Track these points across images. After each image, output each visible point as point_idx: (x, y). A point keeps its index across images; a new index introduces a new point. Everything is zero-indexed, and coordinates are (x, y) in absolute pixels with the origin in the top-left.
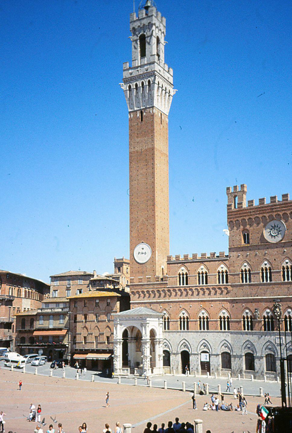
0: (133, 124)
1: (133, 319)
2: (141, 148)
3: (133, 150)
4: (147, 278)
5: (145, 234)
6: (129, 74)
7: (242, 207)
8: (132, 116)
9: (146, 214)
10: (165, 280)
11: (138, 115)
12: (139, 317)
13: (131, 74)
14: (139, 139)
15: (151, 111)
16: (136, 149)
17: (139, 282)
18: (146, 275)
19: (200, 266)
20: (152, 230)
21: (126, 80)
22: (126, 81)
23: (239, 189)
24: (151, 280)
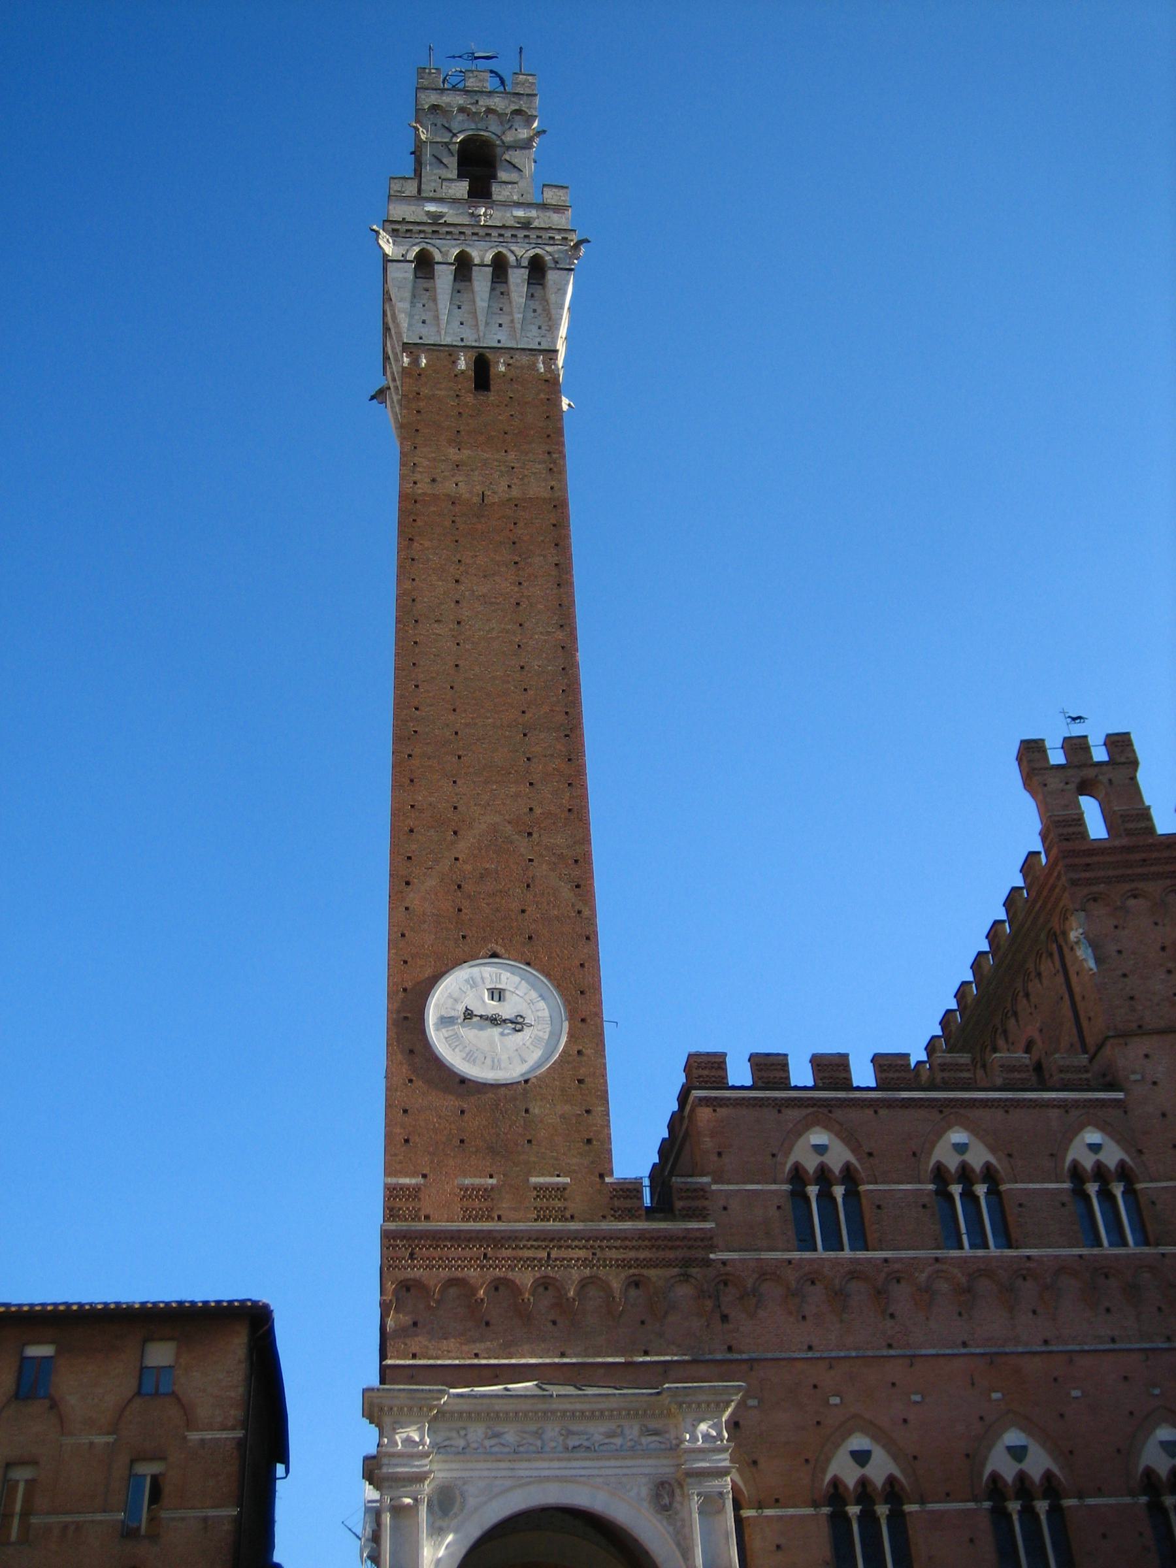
0: (425, 391)
1: (573, 1442)
2: (479, 489)
3: (423, 487)
4: (538, 1188)
5: (515, 906)
6: (422, 213)
7: (1151, 829)
8: (424, 362)
9: (517, 795)
10: (690, 1215)
11: (462, 365)
12: (633, 1430)
13: (436, 217)
14: (466, 452)
15: (541, 368)
16: (449, 487)
17: (465, 1219)
18: (529, 1174)
19: (940, 1133)
20: (566, 892)
21: (408, 231)
22: (399, 230)
23: (1100, 754)
24: (575, 1205)
